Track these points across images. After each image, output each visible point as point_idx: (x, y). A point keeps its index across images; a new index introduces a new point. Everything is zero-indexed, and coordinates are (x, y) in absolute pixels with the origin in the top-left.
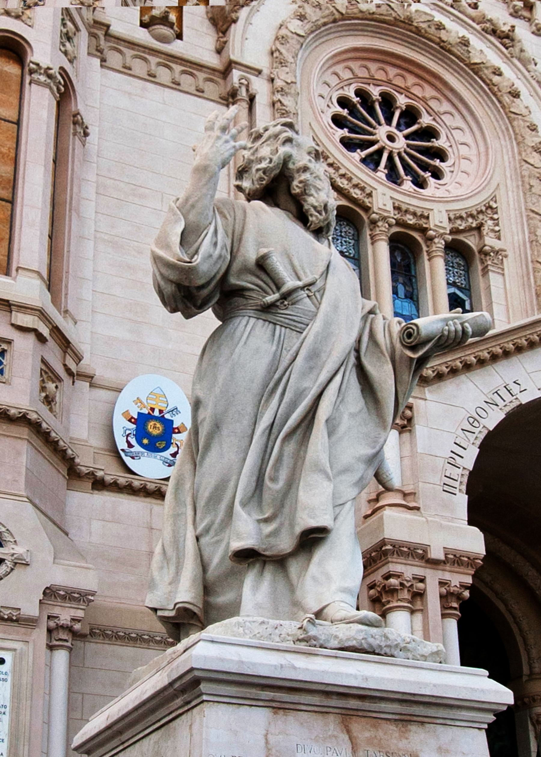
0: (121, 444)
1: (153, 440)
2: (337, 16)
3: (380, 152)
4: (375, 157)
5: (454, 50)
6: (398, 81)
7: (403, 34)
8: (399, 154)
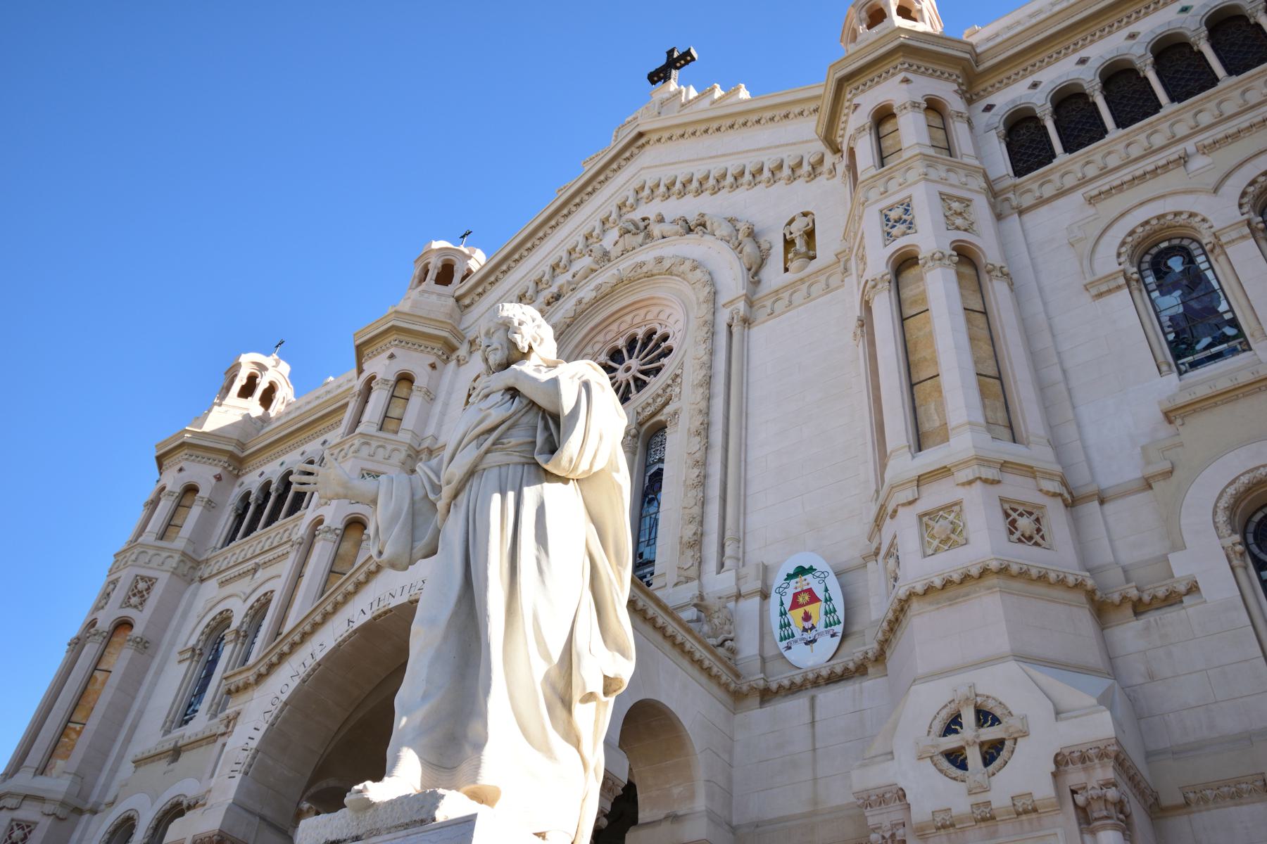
2: (568, 321)
3: (636, 379)
4: (639, 383)
5: (655, 272)
6: (637, 320)
7: (625, 289)
8: (643, 372)
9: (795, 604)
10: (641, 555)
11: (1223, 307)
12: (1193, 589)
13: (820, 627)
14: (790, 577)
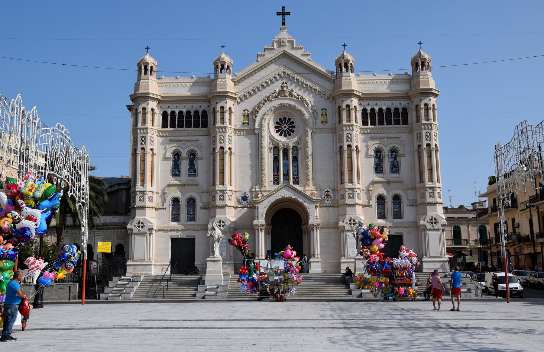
0: (241, 201)
1: (245, 199)
9: (326, 195)
10: (294, 173)
11: (382, 165)
12: (371, 206)
13: (329, 199)
14: (326, 191)
